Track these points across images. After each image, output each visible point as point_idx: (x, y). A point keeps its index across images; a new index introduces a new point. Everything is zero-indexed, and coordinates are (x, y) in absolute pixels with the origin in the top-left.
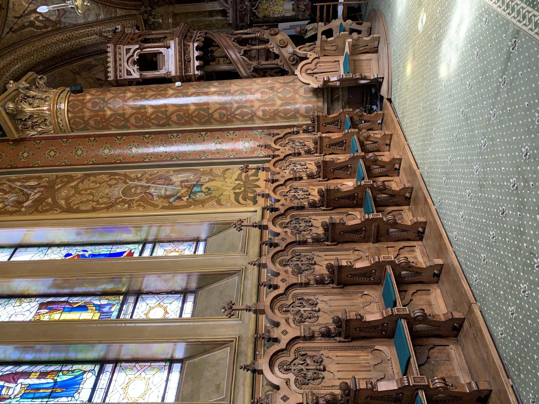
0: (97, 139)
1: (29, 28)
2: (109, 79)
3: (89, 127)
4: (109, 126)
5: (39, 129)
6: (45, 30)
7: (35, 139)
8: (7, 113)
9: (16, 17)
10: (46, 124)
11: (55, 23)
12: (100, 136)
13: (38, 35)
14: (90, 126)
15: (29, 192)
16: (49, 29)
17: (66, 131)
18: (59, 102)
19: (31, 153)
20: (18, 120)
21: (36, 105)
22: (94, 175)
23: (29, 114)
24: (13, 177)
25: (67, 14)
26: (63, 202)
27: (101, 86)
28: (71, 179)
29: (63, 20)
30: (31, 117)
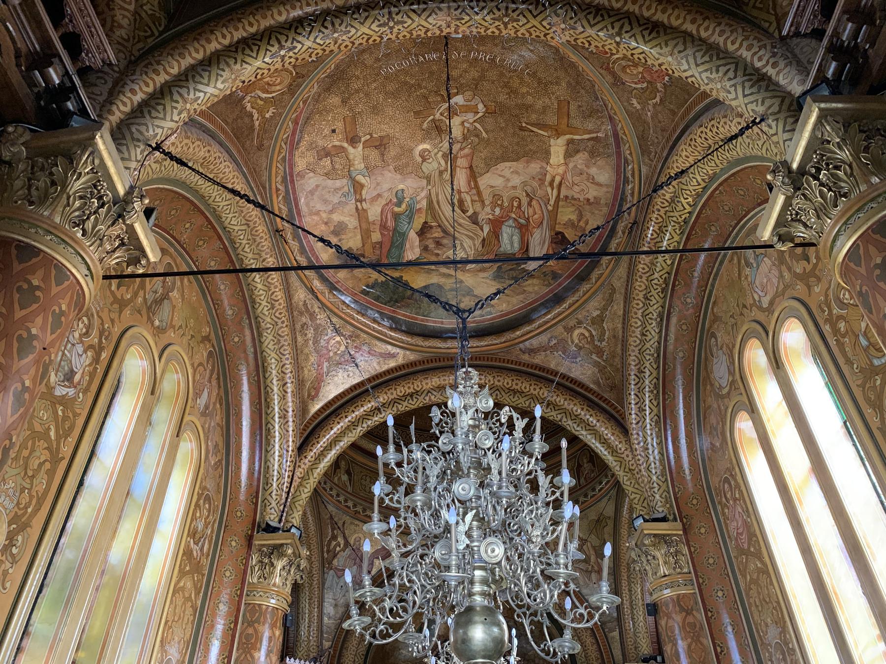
0: (231, 632)
1: (330, 534)
2: (288, 659)
3: (246, 624)
4: (241, 651)
5: (256, 569)
6: (325, 549)
7: (247, 559)
8: (282, 545)
9: (344, 523)
10: (260, 577)
11: (330, 563)
12: (233, 637)
13: (322, 541)
14: (246, 628)
15: (200, 544)
16: (326, 555)
17: (249, 598)
18: (279, 598)
19: (234, 550)
20: (273, 550)
21: (282, 573)
22: (193, 623)
23: (275, 562)
24: (216, 525)
25: (336, 578)
26: (182, 584)
27: (282, 651)
28: (197, 594)
29: (332, 572)
30: (272, 565)
